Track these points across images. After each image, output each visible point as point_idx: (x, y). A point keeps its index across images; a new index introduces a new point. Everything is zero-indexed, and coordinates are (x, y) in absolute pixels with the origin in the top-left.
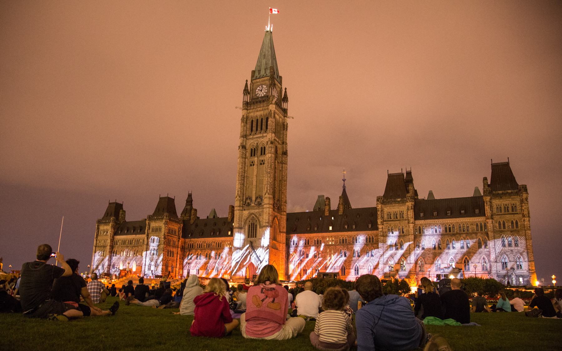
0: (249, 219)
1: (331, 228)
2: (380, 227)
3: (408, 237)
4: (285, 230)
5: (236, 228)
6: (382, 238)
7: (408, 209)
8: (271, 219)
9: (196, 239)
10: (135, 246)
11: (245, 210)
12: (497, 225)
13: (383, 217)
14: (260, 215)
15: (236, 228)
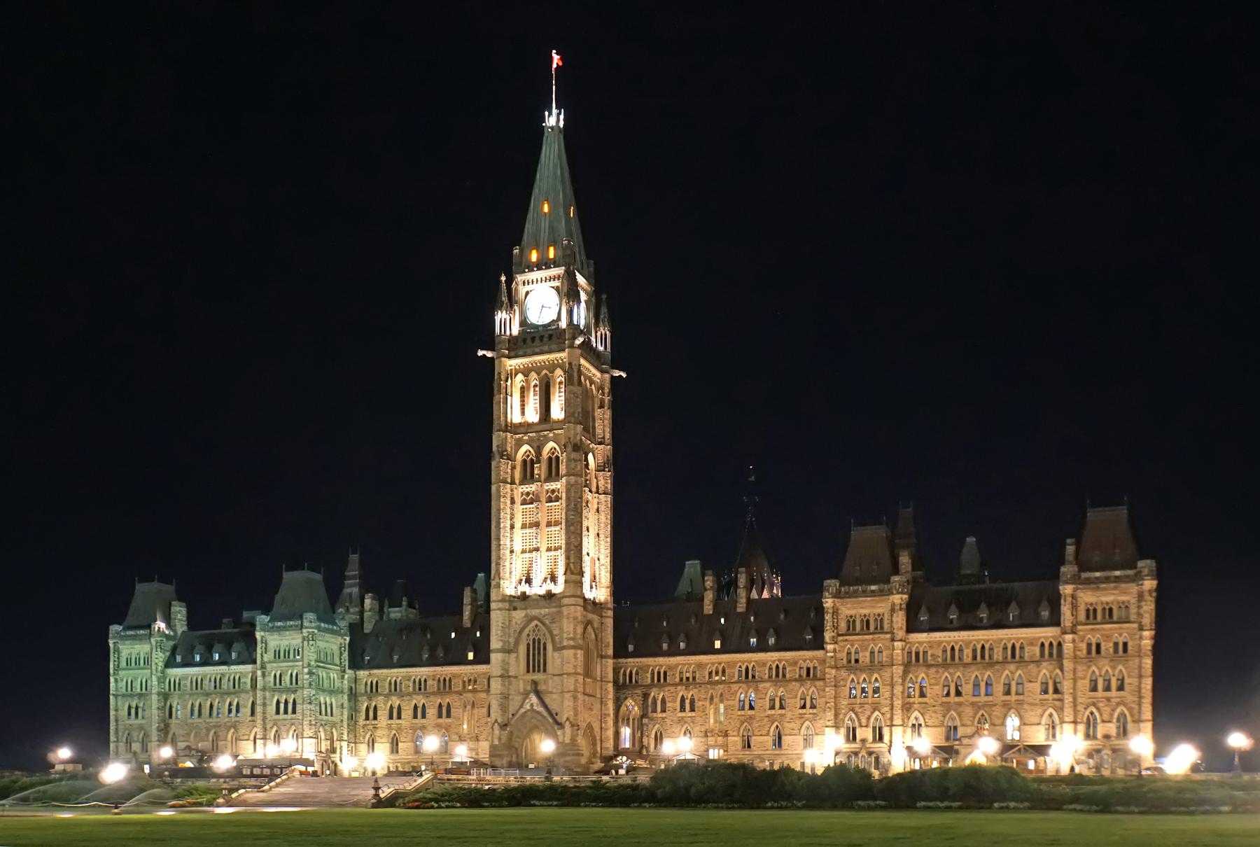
0: (526, 631)
1: (718, 644)
2: (830, 647)
3: (889, 670)
4: (610, 652)
5: (498, 651)
6: (833, 671)
7: (893, 610)
8: (580, 630)
9: (385, 671)
10: (229, 694)
11: (515, 609)
12: (1084, 646)
13: (835, 627)
14: (553, 622)
15: (498, 651)
